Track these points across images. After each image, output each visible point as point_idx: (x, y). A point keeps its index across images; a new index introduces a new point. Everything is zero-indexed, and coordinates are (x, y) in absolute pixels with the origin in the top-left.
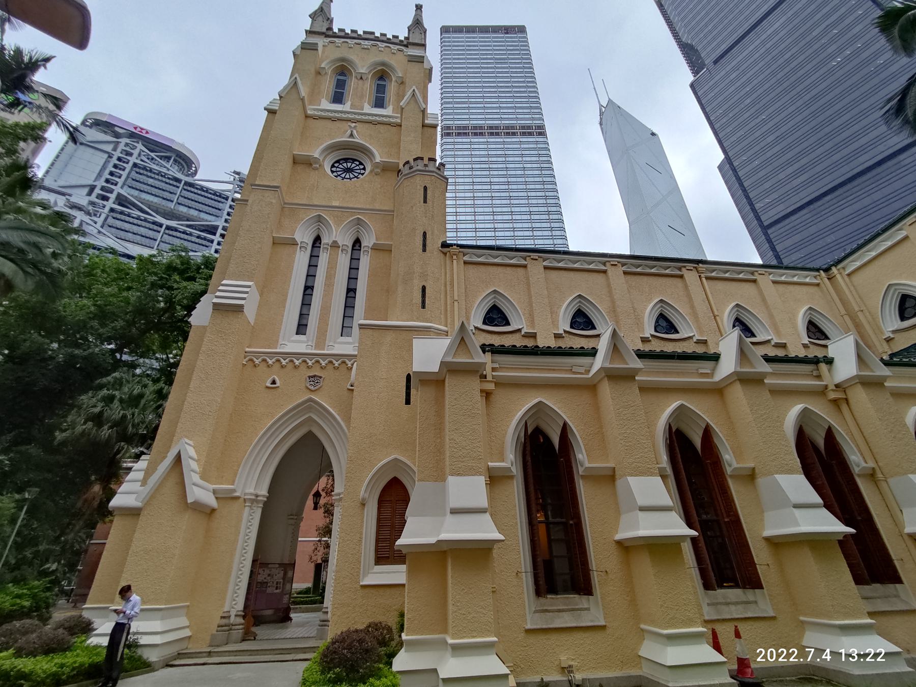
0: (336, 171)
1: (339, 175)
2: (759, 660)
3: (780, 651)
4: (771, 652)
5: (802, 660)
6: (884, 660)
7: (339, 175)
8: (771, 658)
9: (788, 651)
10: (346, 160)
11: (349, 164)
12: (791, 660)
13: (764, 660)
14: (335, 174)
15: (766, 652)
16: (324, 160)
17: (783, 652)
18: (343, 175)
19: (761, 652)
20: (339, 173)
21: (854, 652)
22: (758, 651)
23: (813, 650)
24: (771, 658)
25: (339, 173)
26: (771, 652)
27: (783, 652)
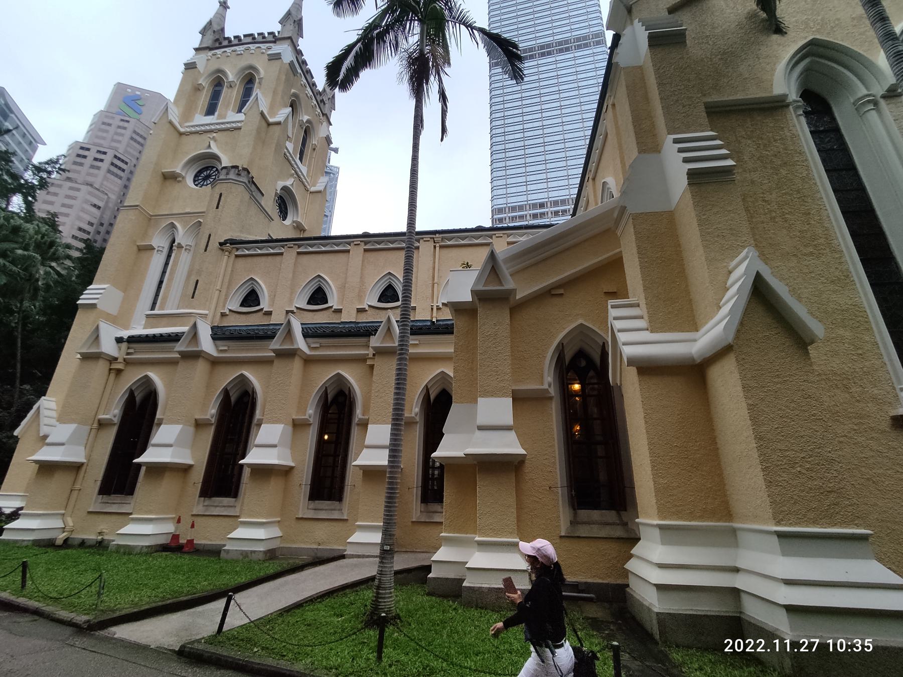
0: (199, 183)
1: (203, 185)
2: (726, 650)
3: (747, 642)
4: (739, 643)
5: (796, 650)
6: (807, 650)
7: (203, 185)
8: (739, 648)
10: (206, 169)
11: (205, 173)
12: (758, 650)
13: (732, 650)
14: (199, 185)
16: (186, 174)
17: (750, 642)
18: (205, 183)
20: (201, 183)
21: (858, 643)
22: (726, 642)
24: (739, 647)
25: (201, 183)
26: (739, 643)
27: (750, 642)
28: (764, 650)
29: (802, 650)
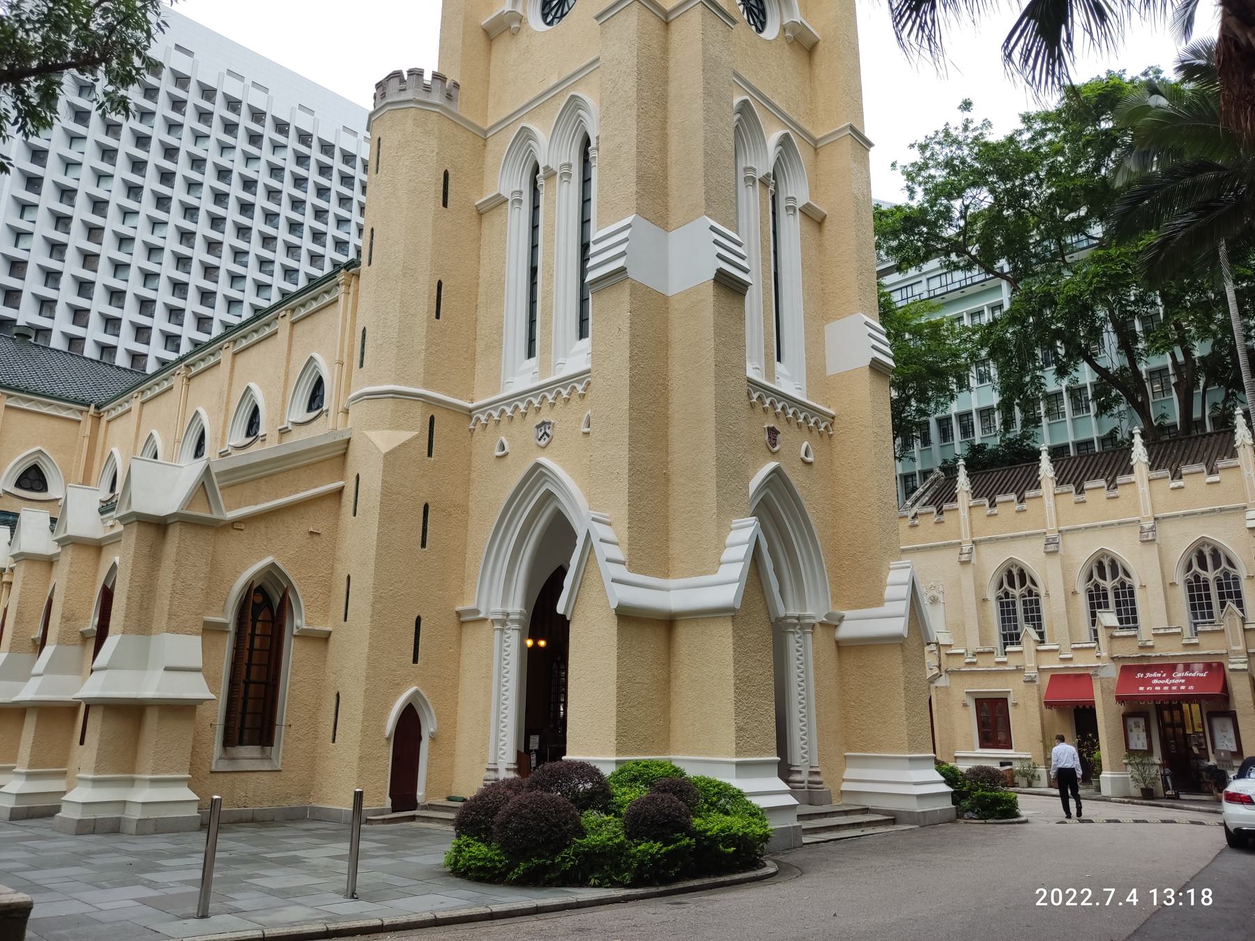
2: (1038, 903)
3: (1067, 892)
8: (1056, 900)
9: (1078, 892)
12: (1083, 903)
13: (1046, 904)
15: (1049, 894)
17: (1071, 893)
19: (1041, 893)
22: (1037, 892)
23: (1113, 890)
24: (1056, 900)
27: (1071, 893)
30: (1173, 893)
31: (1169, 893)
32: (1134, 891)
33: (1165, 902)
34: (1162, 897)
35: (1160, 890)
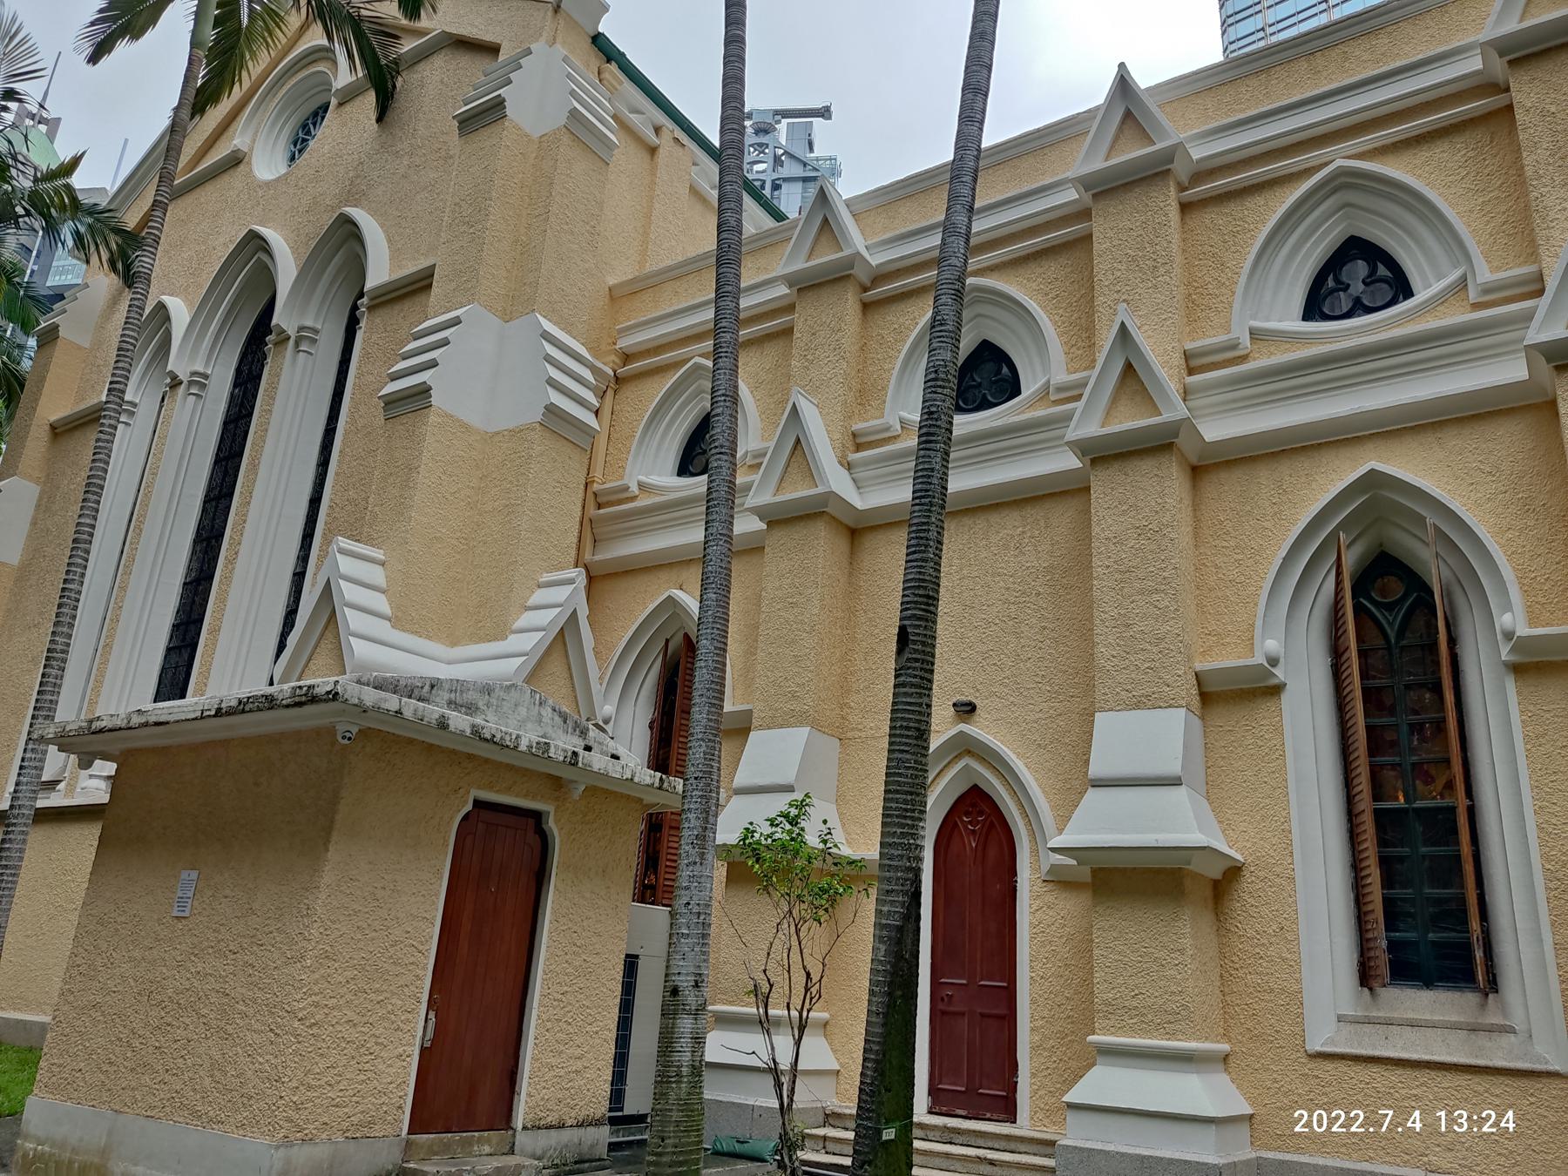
2: (1297, 1129)
8: (1320, 1125)
12: (1353, 1129)
13: (1307, 1130)
15: (1310, 1116)
17: (1338, 1117)
22: (1296, 1115)
23: (1391, 1113)
24: (1320, 1125)
28: (1363, 1130)
29: (1485, 1129)
30: (1465, 1117)
31: (1461, 1116)
32: (1417, 1114)
33: (1456, 1128)
34: (1452, 1121)
35: (1449, 1113)
